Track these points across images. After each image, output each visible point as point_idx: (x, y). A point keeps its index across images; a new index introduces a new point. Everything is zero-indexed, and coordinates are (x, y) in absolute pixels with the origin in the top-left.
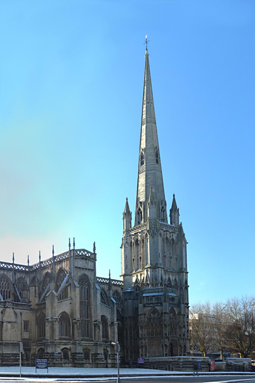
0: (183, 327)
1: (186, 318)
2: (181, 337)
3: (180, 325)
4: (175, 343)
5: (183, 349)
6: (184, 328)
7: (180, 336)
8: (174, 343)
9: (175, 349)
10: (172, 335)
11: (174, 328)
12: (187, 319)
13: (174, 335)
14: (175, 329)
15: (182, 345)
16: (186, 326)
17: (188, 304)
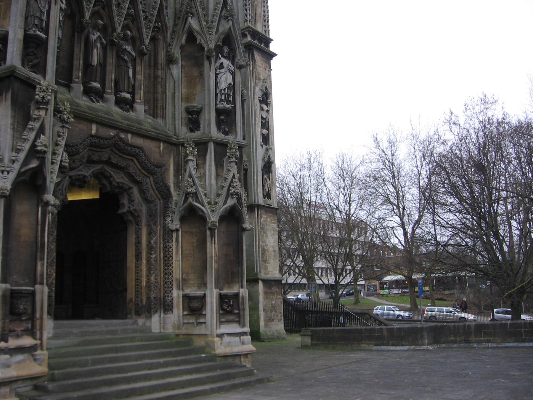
0: (219, 49)
1: (257, 101)
2: (197, 135)
3: (191, 37)
4: (142, 192)
5: (213, 249)
6: (226, 62)
7: (194, 119)
8: (135, 191)
9: (150, 248)
10: (116, 110)
11: (142, 54)
12: (265, 107)
13: (140, 108)
14: (154, 65)
15: (206, 209)
16: (259, 139)
17: (268, 41)
